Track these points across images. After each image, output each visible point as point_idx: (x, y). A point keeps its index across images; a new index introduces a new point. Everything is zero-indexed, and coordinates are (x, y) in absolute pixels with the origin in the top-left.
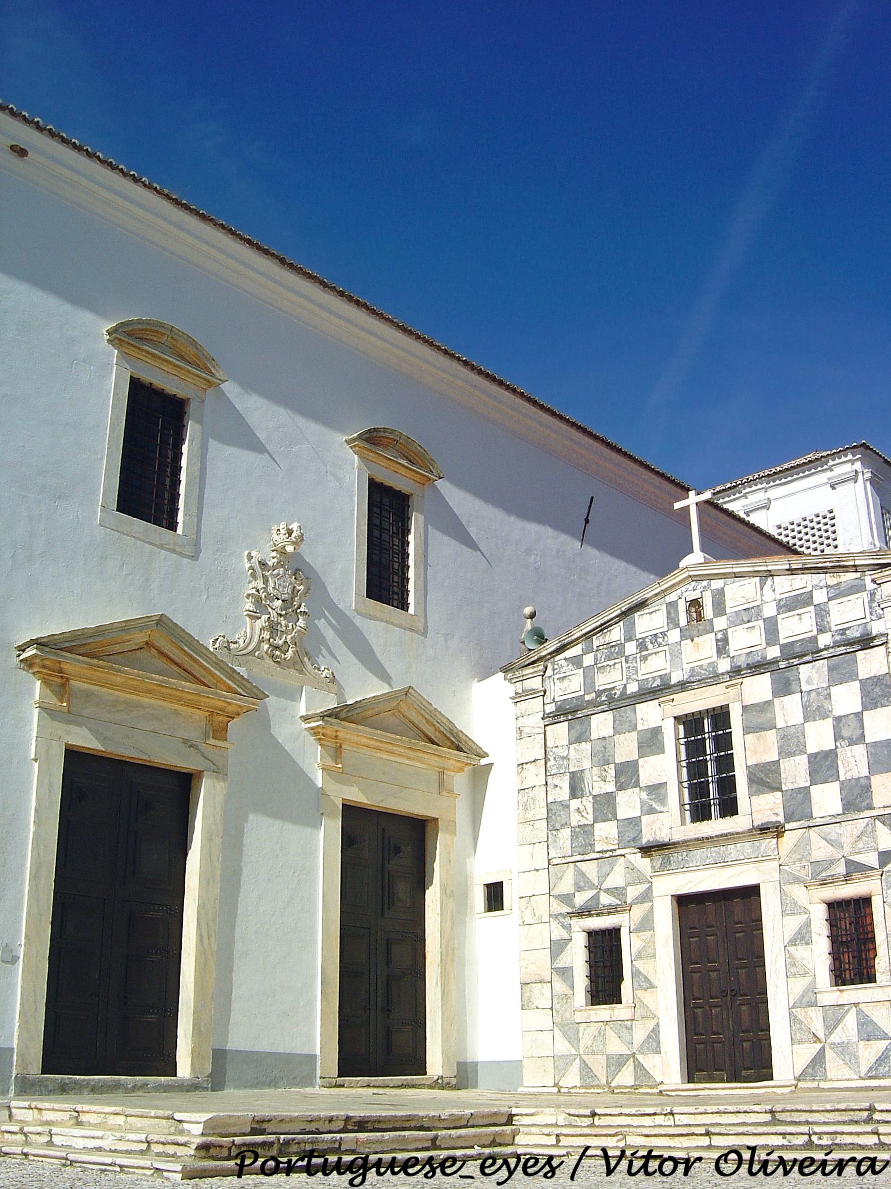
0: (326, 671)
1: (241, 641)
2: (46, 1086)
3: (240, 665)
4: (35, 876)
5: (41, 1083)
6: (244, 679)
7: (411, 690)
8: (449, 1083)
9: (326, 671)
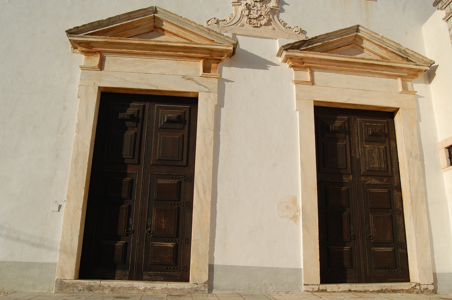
0: (296, 28)
1: (228, 19)
2: (78, 287)
3: (227, 32)
4: (75, 161)
5: (74, 285)
6: (217, 33)
7: (360, 28)
8: (427, 289)
9: (296, 28)
